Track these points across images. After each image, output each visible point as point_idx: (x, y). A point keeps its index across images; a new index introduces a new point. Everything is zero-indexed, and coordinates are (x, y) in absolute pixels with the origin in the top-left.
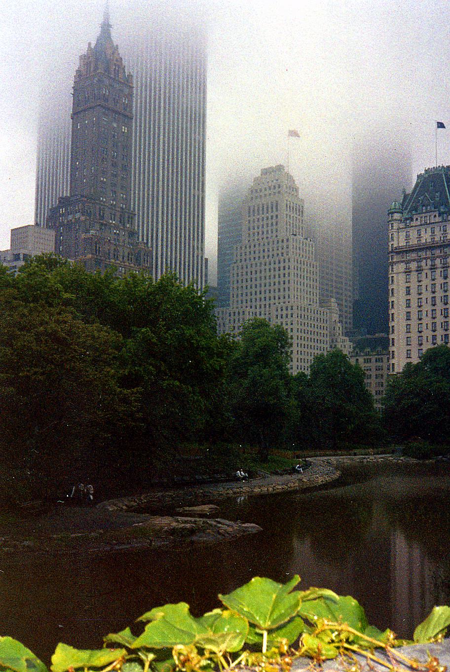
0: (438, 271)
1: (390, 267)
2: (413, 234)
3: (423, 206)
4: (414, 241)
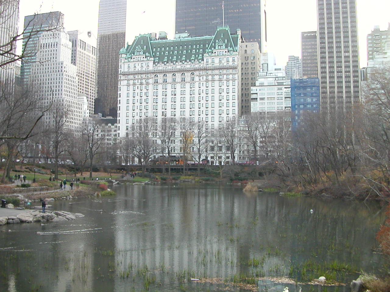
0: (144, 86)
1: (119, 82)
2: (132, 65)
3: (137, 52)
4: (132, 70)
